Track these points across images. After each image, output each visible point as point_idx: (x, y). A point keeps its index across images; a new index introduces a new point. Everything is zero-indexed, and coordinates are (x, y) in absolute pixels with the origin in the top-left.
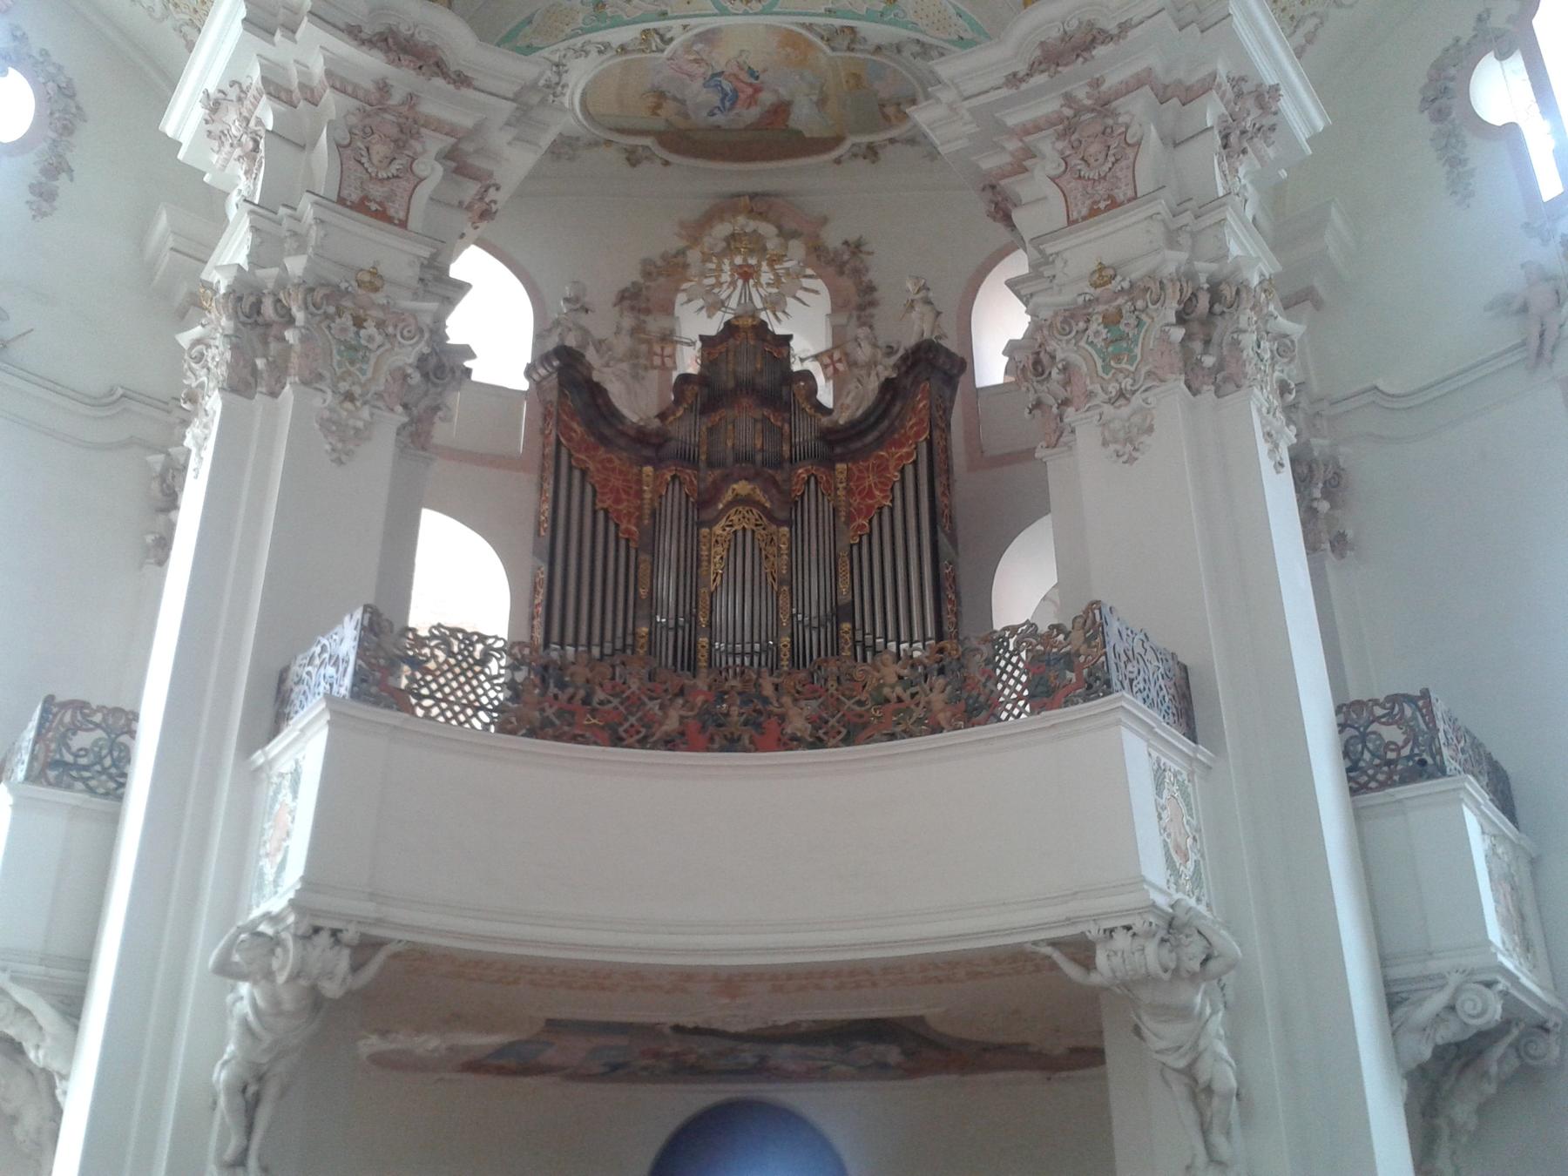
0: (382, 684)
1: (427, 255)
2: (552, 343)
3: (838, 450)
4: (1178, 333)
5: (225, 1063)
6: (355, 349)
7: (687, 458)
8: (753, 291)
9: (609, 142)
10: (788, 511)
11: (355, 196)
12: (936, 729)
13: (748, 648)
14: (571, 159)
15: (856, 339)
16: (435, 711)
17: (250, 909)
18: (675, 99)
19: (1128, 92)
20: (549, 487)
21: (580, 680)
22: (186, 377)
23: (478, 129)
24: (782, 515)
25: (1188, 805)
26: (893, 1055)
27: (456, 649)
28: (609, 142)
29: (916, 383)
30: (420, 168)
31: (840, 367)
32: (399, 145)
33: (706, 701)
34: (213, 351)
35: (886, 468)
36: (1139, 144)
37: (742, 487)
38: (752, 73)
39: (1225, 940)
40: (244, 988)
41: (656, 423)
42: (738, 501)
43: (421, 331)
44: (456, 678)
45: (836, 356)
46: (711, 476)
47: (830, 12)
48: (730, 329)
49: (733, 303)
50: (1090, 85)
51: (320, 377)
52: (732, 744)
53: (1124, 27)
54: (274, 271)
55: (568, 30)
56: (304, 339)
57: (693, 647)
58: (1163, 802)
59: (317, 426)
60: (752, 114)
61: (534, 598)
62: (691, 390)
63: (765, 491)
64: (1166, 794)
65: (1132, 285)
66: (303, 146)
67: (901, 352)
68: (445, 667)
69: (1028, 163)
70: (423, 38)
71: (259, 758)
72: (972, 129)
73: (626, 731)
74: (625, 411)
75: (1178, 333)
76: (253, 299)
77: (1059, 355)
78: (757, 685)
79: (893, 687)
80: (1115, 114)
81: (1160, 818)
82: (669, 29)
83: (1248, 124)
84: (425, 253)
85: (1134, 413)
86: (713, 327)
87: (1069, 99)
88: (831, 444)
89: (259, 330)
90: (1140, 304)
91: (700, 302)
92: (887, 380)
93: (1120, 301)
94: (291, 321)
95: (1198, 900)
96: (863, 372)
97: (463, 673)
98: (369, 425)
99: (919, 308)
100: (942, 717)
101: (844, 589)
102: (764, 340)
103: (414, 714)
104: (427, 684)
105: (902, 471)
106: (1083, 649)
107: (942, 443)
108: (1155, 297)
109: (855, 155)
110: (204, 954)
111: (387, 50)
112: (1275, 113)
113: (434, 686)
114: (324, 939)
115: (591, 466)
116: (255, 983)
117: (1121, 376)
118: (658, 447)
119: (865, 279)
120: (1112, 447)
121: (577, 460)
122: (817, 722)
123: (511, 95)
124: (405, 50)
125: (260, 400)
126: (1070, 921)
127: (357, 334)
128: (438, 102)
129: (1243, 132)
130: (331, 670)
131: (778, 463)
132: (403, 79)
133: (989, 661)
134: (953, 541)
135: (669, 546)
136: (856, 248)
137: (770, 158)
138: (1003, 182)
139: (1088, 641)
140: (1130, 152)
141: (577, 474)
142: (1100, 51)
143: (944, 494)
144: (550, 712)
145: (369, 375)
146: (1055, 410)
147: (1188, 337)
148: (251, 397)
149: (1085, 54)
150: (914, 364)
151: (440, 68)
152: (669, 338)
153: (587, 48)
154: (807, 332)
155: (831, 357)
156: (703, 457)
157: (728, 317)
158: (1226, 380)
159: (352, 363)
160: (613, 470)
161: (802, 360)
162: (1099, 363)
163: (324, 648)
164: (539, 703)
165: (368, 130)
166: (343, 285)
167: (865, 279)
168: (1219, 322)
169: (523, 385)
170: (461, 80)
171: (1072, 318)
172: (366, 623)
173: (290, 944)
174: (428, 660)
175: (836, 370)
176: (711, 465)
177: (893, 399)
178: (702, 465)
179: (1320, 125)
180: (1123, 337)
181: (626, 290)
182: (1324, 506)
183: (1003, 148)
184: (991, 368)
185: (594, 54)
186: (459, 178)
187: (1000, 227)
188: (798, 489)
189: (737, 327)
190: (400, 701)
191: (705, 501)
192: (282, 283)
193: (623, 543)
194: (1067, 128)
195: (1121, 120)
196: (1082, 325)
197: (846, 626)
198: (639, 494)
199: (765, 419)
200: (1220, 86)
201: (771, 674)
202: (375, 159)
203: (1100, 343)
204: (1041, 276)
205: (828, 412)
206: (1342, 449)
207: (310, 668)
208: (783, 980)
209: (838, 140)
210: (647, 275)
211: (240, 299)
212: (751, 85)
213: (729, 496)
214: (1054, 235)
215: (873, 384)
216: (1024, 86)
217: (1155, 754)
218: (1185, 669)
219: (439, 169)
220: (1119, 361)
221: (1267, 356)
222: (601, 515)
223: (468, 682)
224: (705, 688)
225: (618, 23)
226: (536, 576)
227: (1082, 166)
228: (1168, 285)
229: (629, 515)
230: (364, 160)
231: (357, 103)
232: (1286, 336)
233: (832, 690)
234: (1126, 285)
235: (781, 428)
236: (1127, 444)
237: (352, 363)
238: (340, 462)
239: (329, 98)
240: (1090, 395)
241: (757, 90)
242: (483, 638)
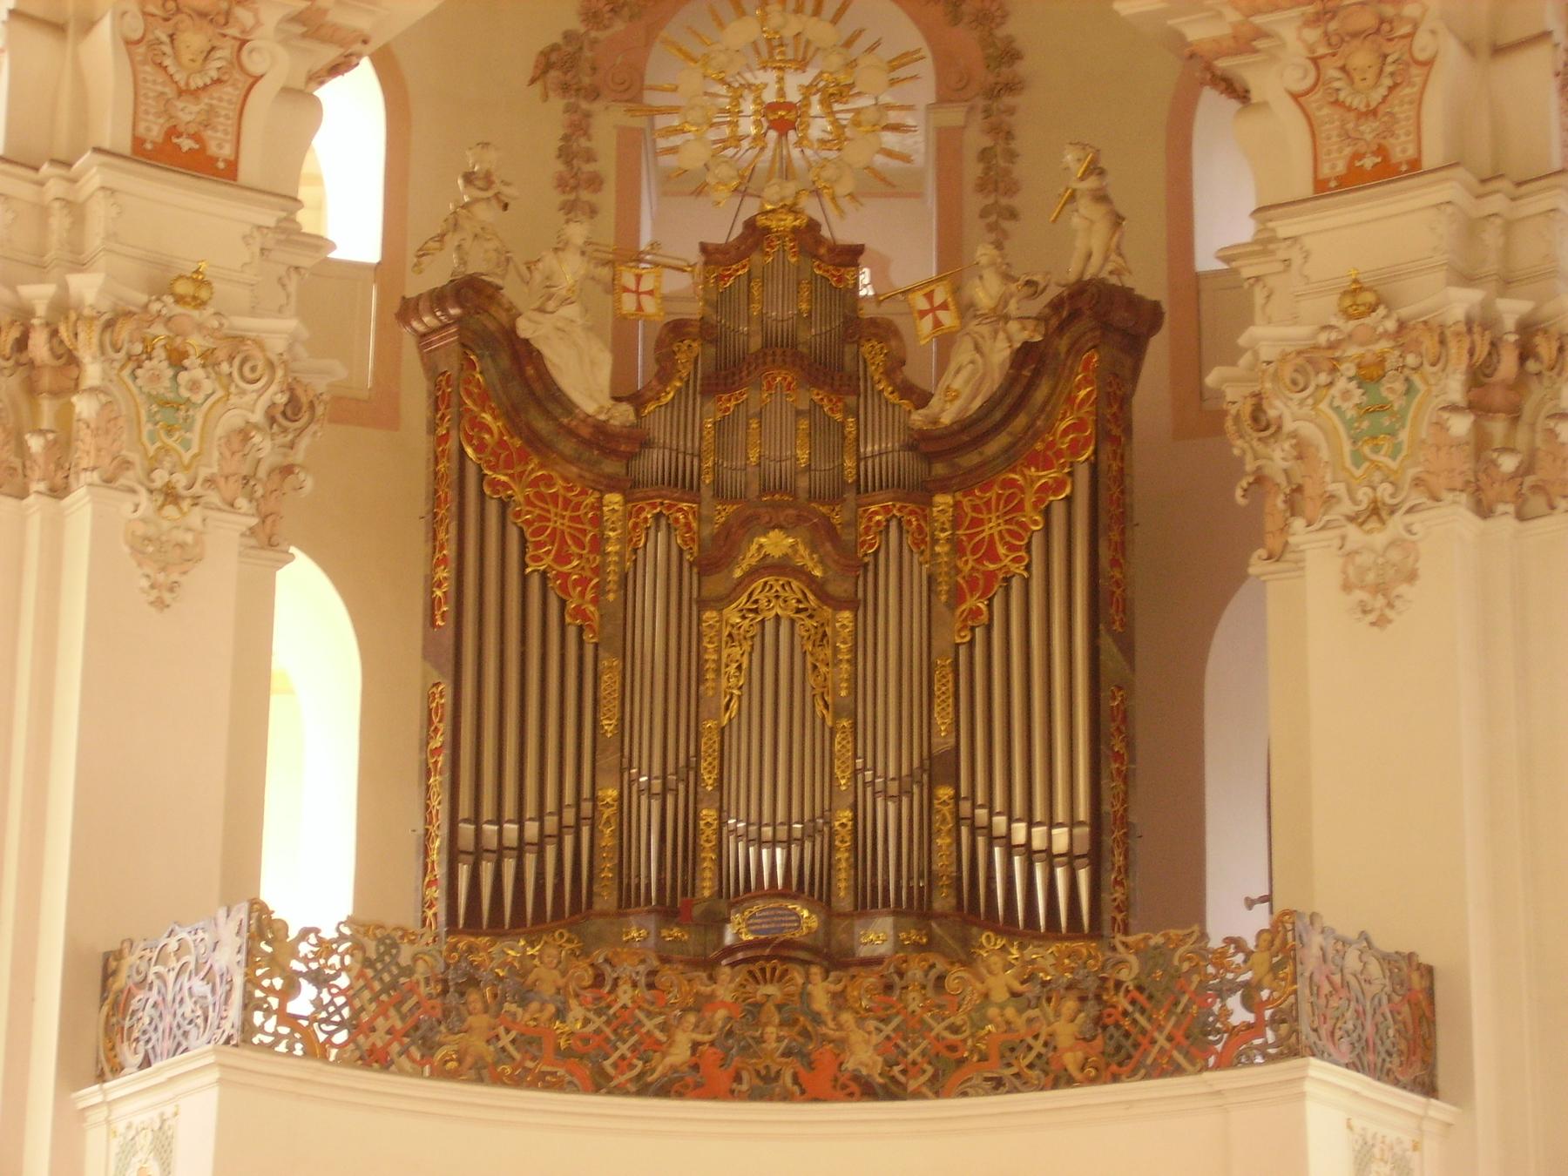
3: (940, 469)
4: (1461, 425)
8: (795, 153)
10: (846, 580)
11: (154, 130)
12: (1062, 1079)
13: (782, 833)
20: (448, 535)
21: (547, 990)
24: (839, 588)
29: (1075, 349)
33: (730, 1018)
35: (1020, 507)
36: (1428, 64)
37: (775, 543)
41: (623, 415)
43: (271, 365)
46: (723, 514)
48: (755, 234)
51: (127, 464)
52: (766, 1088)
59: (126, 549)
62: (688, 353)
63: (813, 547)
65: (1402, 325)
74: (576, 396)
76: (15, 333)
77: (1289, 426)
78: (805, 996)
79: (1002, 1007)
84: (270, 221)
85: (1392, 544)
92: (1026, 344)
93: (1384, 345)
96: (985, 330)
100: (1071, 1060)
101: (942, 724)
102: (816, 257)
105: (1047, 514)
106: (1267, 979)
115: (519, 494)
117: (1377, 477)
118: (630, 457)
119: (1000, 33)
120: (1359, 595)
121: (495, 484)
122: (892, 1055)
125: (36, 503)
127: (175, 376)
130: (201, 987)
131: (836, 498)
134: (1127, 647)
143: (1115, 563)
144: (505, 1040)
145: (195, 450)
148: (22, 494)
150: (1075, 315)
155: (929, 296)
160: (555, 496)
162: (1347, 448)
167: (1000, 33)
168: (1537, 392)
174: (337, 975)
176: (719, 493)
177: (1031, 386)
178: (707, 493)
180: (1383, 408)
181: (555, 48)
189: (767, 230)
191: (712, 559)
192: (62, 307)
193: (572, 633)
196: (1323, 378)
197: (945, 793)
198: (598, 544)
201: (826, 978)
202: (186, 57)
207: (159, 968)
213: (750, 557)
215: (1000, 353)
219: (281, 52)
220: (1376, 449)
222: (535, 583)
226: (431, 697)
229: (583, 582)
230: (167, 62)
234: (1391, 325)
235: (843, 425)
236: (1379, 592)
237: (170, 431)
238: (160, 604)
240: (1330, 499)
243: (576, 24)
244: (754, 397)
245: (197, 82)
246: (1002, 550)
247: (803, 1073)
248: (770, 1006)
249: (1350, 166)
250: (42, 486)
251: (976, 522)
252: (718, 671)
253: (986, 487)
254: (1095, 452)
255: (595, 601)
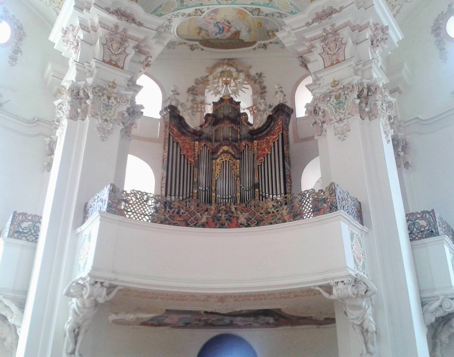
0: (115, 208)
1: (130, 77)
2: (167, 104)
3: (255, 137)
4: (358, 101)
5: (69, 323)
6: (108, 106)
7: (209, 139)
8: (229, 88)
9: (185, 43)
11: (108, 60)
12: (284, 221)
13: (227, 197)
14: (173, 48)
15: (260, 103)
16: (132, 216)
17: (76, 276)
18: (205, 30)
19: (342, 28)
20: (167, 148)
21: (176, 206)
22: (57, 115)
23: (145, 40)
25: (361, 244)
26: (271, 320)
27: (138, 197)
28: (185, 43)
29: (278, 116)
30: (127, 51)
31: (255, 111)
32: (121, 44)
33: (214, 213)
34: (65, 107)
35: (269, 142)
37: (225, 148)
38: (228, 22)
39: (372, 286)
40: (74, 300)
42: (224, 152)
43: (128, 101)
44: (138, 206)
45: (254, 108)
46: (216, 144)
47: (252, 4)
48: (222, 100)
49: (223, 92)
50: (331, 26)
51: (97, 114)
52: (222, 226)
53: (341, 8)
54: (84, 82)
55: (172, 9)
56: (92, 103)
57: (210, 196)
58: (353, 243)
59: (96, 129)
60: (228, 35)
61: (162, 181)
62: (210, 119)
63: (232, 149)
64: (354, 241)
66: (92, 44)
67: (274, 107)
68: (135, 203)
69: (312, 50)
70: (128, 11)
71: (79, 230)
72: (295, 39)
73: (190, 222)
74: (190, 125)
75: (358, 101)
77: (322, 108)
78: (230, 208)
79: (271, 209)
80: (339, 35)
81: (352, 248)
82: (203, 9)
83: (379, 38)
84: (129, 77)
85: (344, 125)
86: (217, 99)
87: (324, 30)
88: (252, 135)
89: (79, 100)
90: (346, 92)
91: (213, 92)
93: (340, 91)
94: (88, 97)
95: (364, 273)
96: (262, 113)
97: (141, 204)
98: (112, 129)
99: (279, 93)
100: (286, 218)
101: (256, 179)
102: (232, 103)
103: (126, 217)
104: (130, 208)
105: (274, 143)
106: (329, 197)
107: (286, 135)
108: (351, 90)
109: (260, 47)
110: (62, 290)
111: (118, 15)
112: (387, 34)
113: (132, 208)
114: (98, 285)
115: (180, 141)
116: (78, 298)
117: (340, 114)
118: (201, 135)
119: (263, 85)
120: (338, 136)
121: (175, 140)
122: (248, 219)
123: (155, 29)
124: (123, 16)
125: (79, 121)
126: (325, 280)
127: (108, 101)
128: (133, 31)
129: (378, 40)
130: (100, 203)
131: (236, 141)
132: (123, 24)
133: (300, 201)
134: (290, 164)
135: (203, 166)
136: (260, 75)
137: (234, 48)
138: (304, 55)
139: (330, 195)
140: (343, 46)
141: (175, 144)
142: (334, 15)
143: (287, 150)
144: (167, 216)
145: (112, 113)
146: (320, 124)
147: (361, 102)
149: (330, 17)
150: (278, 110)
151: (134, 21)
152: (203, 103)
153: (178, 14)
154: (245, 100)
155: (252, 108)
156: (213, 139)
157: (221, 96)
158: (372, 115)
159: (107, 110)
160: (186, 142)
161: (244, 109)
162: (334, 110)
163: (98, 197)
164: (164, 213)
165: (112, 40)
166: (104, 87)
168: (370, 97)
169: (159, 117)
170: (140, 24)
171: (325, 97)
172: (111, 189)
173: (88, 286)
175: (254, 112)
176: (216, 141)
178: (213, 141)
179: (401, 38)
181: (190, 88)
182: (402, 154)
183: (305, 45)
184: (300, 112)
185: (180, 16)
186: (140, 54)
187: (304, 69)
188: (242, 148)
189: (224, 99)
190: (121, 213)
191: (214, 152)
192: (85, 86)
193: (189, 165)
194: (324, 39)
195: (340, 36)
196: (328, 99)
197: (257, 190)
199: (232, 127)
200: (370, 26)
201: (234, 204)
202: (114, 48)
203: (334, 104)
204: (316, 84)
205: (251, 125)
206: (408, 136)
207: (94, 203)
208: (237, 297)
209: (254, 43)
210: (197, 83)
211: (73, 91)
212: (228, 26)
213: (221, 151)
214: (320, 71)
215: (265, 117)
216: (311, 26)
217: (351, 229)
218: (360, 203)
219: (133, 52)
220: (340, 110)
221: (385, 108)
222: (182, 156)
223: (142, 207)
224: (214, 209)
225: (187, 7)
226: (163, 175)
227: (328, 50)
228: (355, 87)
229: (191, 156)
231: (109, 31)
232: (391, 102)
233: (253, 210)
234: (342, 86)
235: (237, 130)
237: (107, 110)
238: (103, 140)
239: (100, 30)
240: (331, 120)
241: (230, 27)
242: (146, 194)
243: (194, 84)
244: (221, 125)
245: (116, 53)
246: (266, 150)
247: (230, 224)
248: (223, 210)
249: (331, 63)
250: (80, 118)
251: (261, 145)
252: (215, 170)
253: (263, 139)
254: (283, 132)
255: (193, 159)
